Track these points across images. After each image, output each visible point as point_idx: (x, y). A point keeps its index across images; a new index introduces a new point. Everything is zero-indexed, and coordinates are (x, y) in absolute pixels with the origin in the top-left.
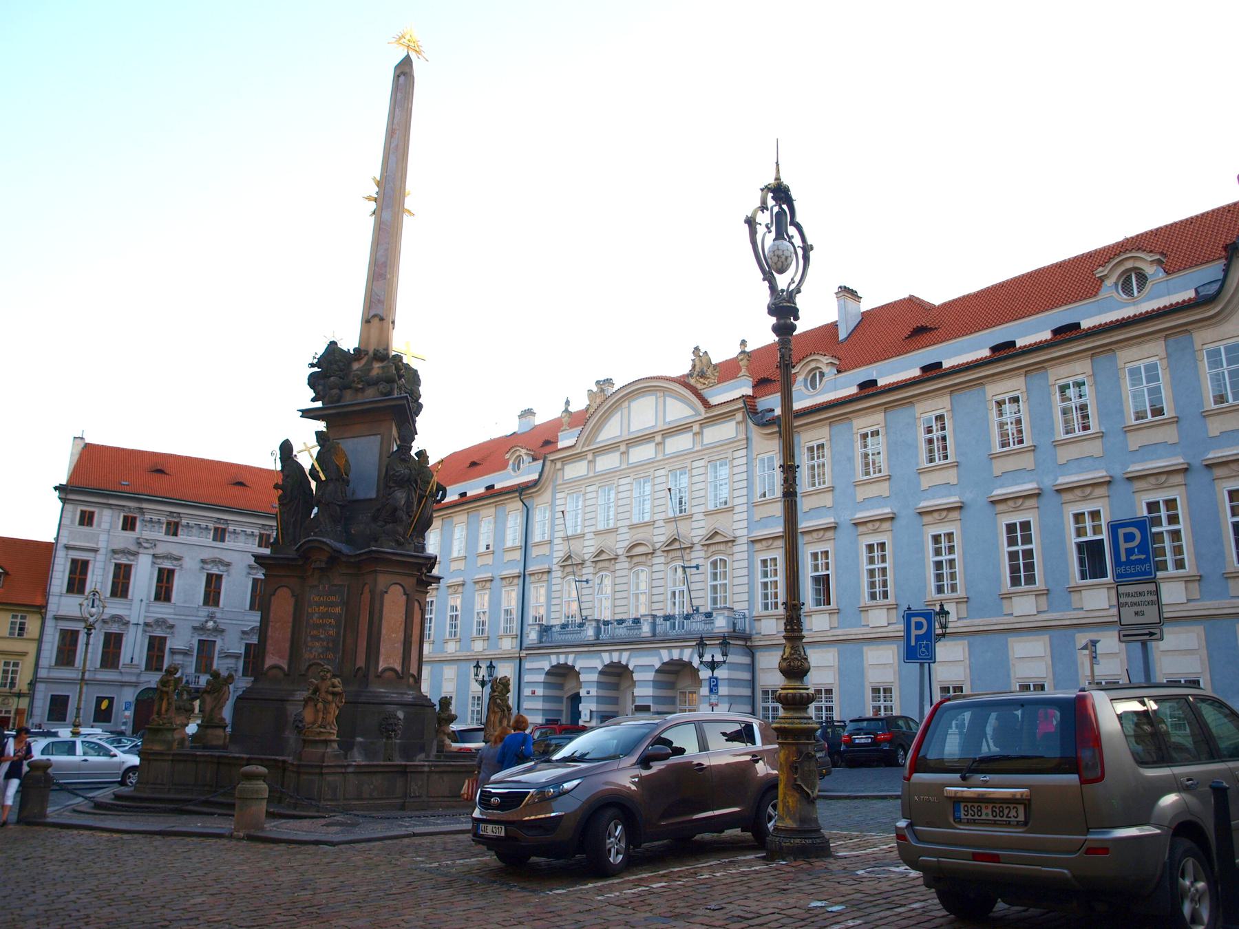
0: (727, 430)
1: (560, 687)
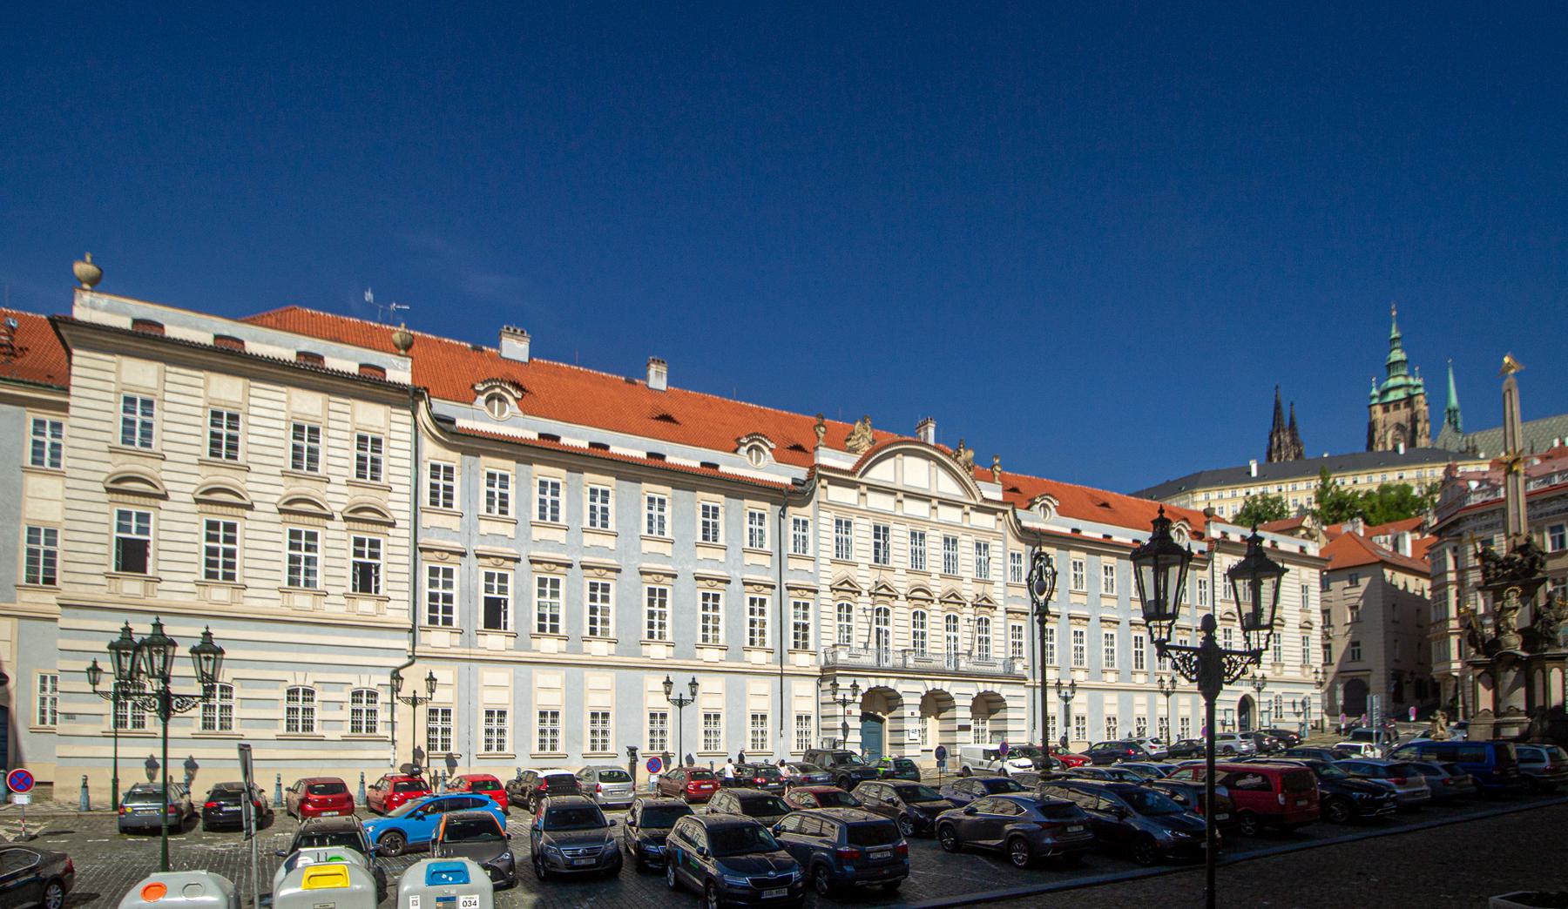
0: (987, 521)
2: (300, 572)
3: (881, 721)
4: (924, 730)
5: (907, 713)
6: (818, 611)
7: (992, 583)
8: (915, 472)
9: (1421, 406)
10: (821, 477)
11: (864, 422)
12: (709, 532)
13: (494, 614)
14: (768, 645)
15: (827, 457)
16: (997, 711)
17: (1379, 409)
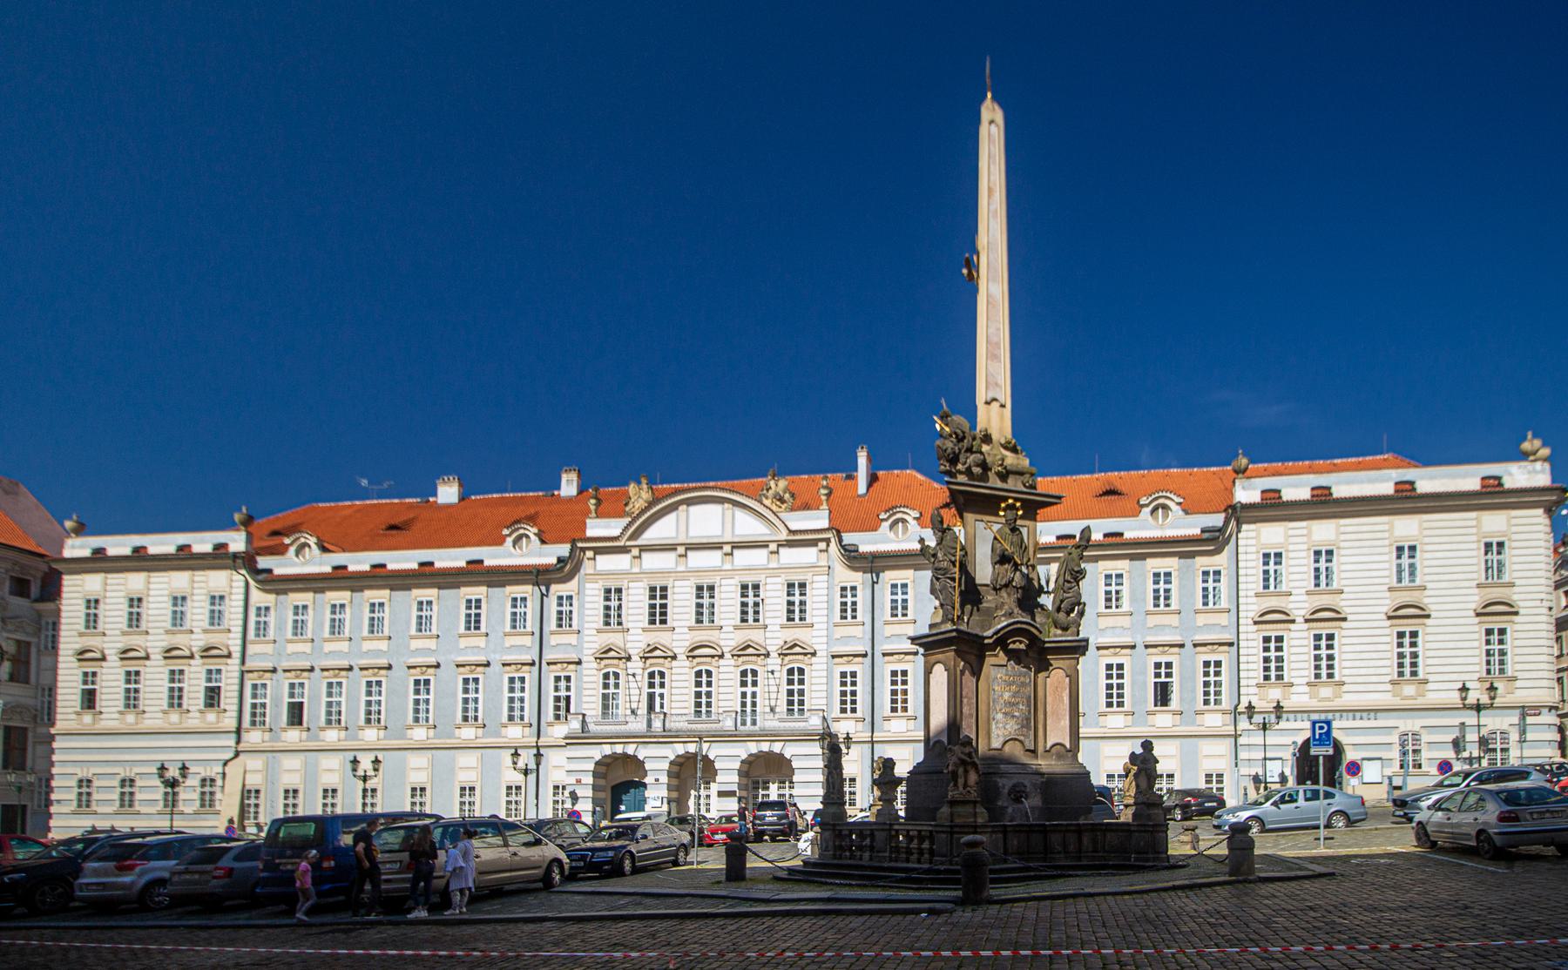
0: (808, 555)
1: (604, 776)
2: (176, 698)
6: (579, 679)
8: (705, 520)
10: (583, 550)
11: (639, 483)
12: (473, 623)
13: (296, 714)
14: (526, 720)
15: (597, 528)
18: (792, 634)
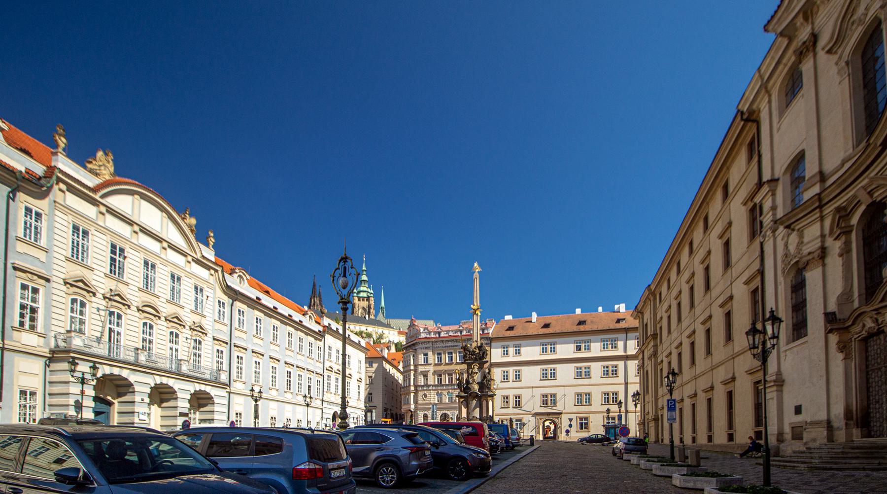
3: (110, 404)
4: (149, 414)
5: (137, 398)
7: (204, 316)
9: (372, 302)
16: (205, 405)
17: (356, 299)
18: (197, 319)
